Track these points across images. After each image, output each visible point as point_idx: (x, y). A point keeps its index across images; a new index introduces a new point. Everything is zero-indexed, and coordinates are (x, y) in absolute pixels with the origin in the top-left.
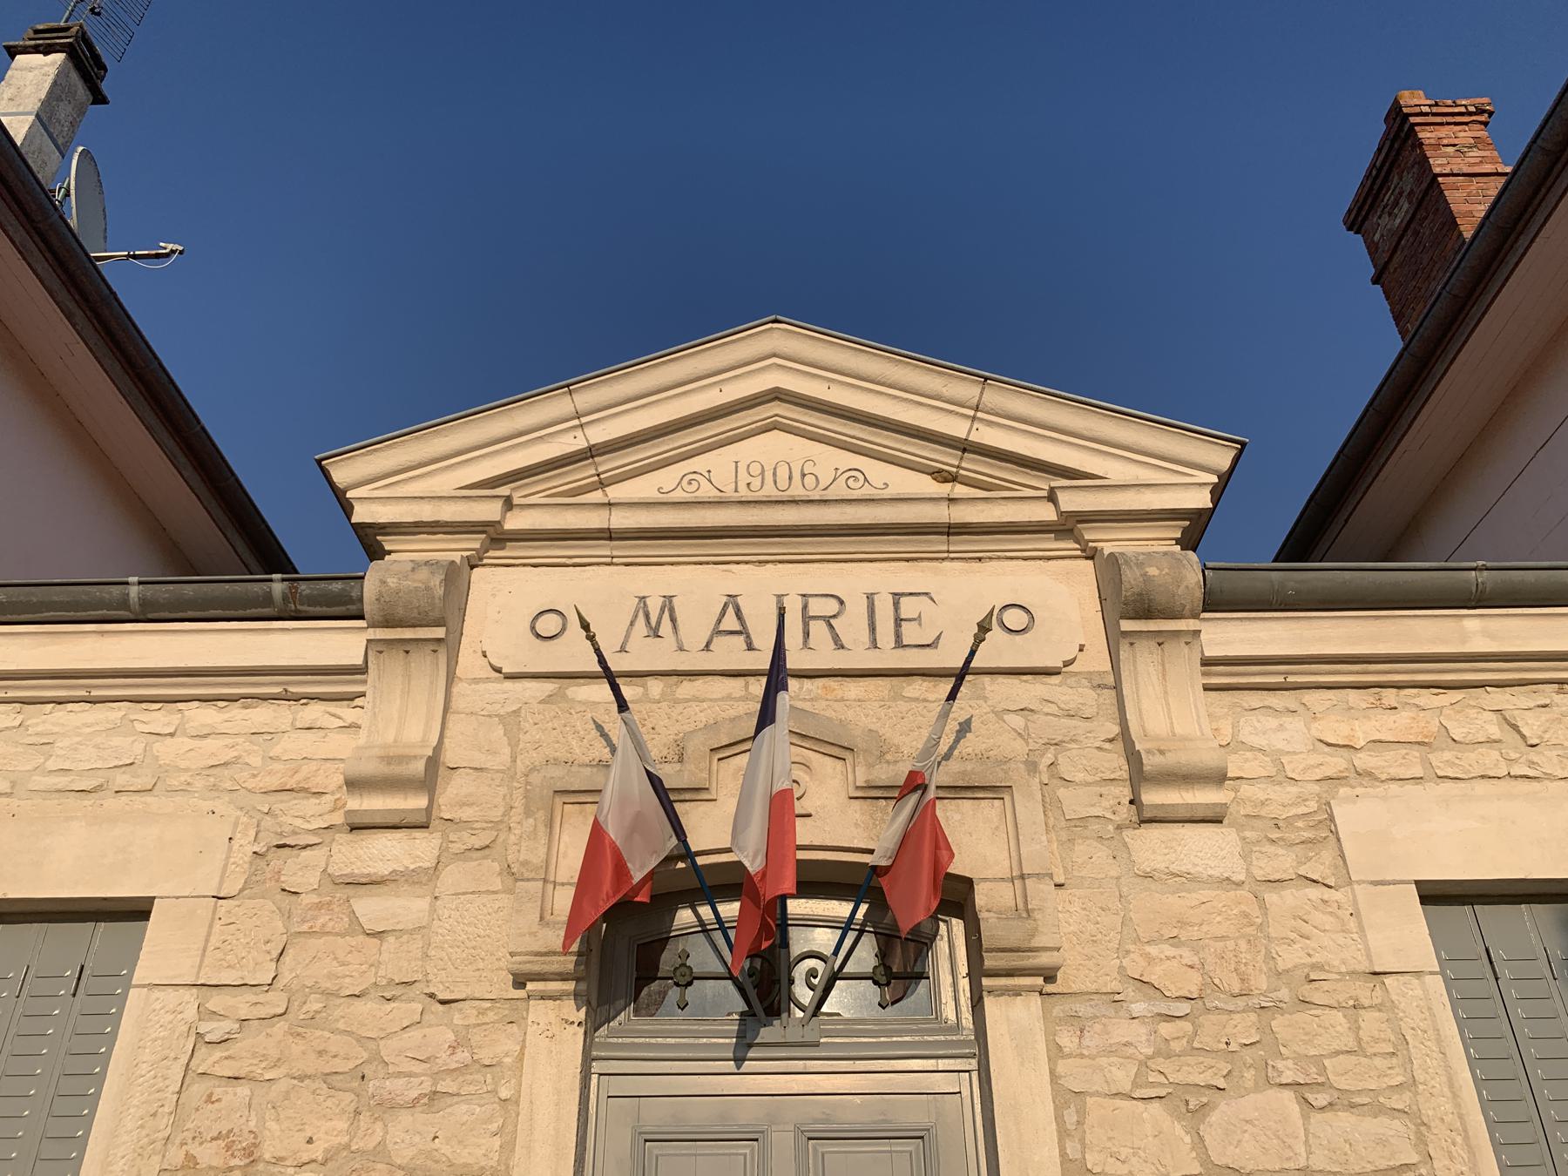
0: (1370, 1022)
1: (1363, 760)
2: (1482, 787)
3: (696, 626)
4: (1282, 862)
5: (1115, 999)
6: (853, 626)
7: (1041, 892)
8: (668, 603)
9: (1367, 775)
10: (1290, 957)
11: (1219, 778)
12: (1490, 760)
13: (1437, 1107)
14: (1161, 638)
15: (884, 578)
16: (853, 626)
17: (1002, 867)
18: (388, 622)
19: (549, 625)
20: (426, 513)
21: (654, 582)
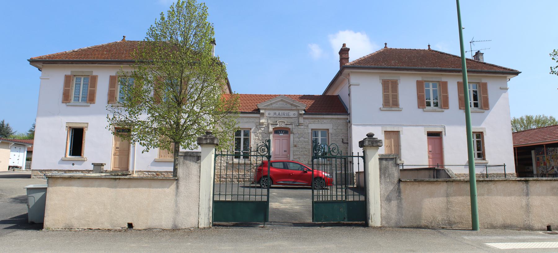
0: (308, 135)
1: (311, 122)
2: (316, 124)
3: (277, 115)
4: (305, 127)
5: (296, 134)
6: (286, 115)
7: (294, 129)
8: (276, 113)
9: (310, 123)
10: (305, 132)
11: (303, 124)
12: (317, 123)
13: (309, 138)
14: (301, 116)
15: (288, 112)
16: (286, 115)
17: (292, 128)
18: (261, 114)
19: (269, 114)
20: (263, 108)
21: (275, 112)
